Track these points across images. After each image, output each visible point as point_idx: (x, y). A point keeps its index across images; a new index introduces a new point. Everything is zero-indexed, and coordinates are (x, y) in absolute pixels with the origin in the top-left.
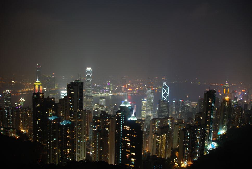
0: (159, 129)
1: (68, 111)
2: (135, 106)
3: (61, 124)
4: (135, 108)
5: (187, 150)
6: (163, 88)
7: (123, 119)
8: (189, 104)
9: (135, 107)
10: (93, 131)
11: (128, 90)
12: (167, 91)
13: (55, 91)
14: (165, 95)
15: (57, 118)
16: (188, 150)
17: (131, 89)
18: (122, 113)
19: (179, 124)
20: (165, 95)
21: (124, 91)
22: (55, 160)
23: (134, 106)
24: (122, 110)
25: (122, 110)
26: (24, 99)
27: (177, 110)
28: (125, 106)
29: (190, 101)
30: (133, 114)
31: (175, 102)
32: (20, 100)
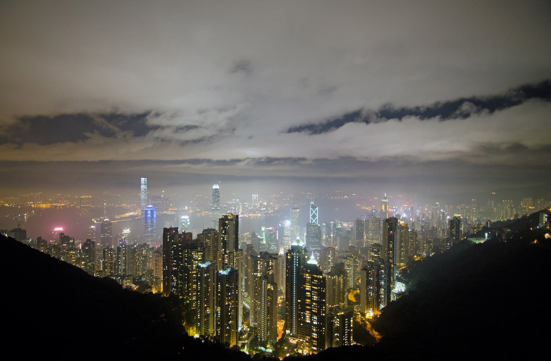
0: (334, 269)
1: (220, 252)
2: (277, 231)
3: (200, 266)
4: (277, 235)
5: (371, 295)
6: (311, 208)
7: (296, 261)
8: (342, 226)
9: (277, 233)
10: (252, 275)
11: (262, 209)
12: (316, 212)
13: (171, 217)
14: (314, 216)
15: (210, 264)
16: (373, 295)
17: (265, 209)
18: (295, 254)
19: (348, 258)
20: (314, 216)
21: (257, 211)
22: (208, 321)
23: (276, 232)
24: (295, 250)
25: (295, 250)
26: (129, 230)
27: (328, 234)
28: (298, 245)
29: (342, 222)
30: (312, 255)
31: (325, 224)
32: (124, 231)
